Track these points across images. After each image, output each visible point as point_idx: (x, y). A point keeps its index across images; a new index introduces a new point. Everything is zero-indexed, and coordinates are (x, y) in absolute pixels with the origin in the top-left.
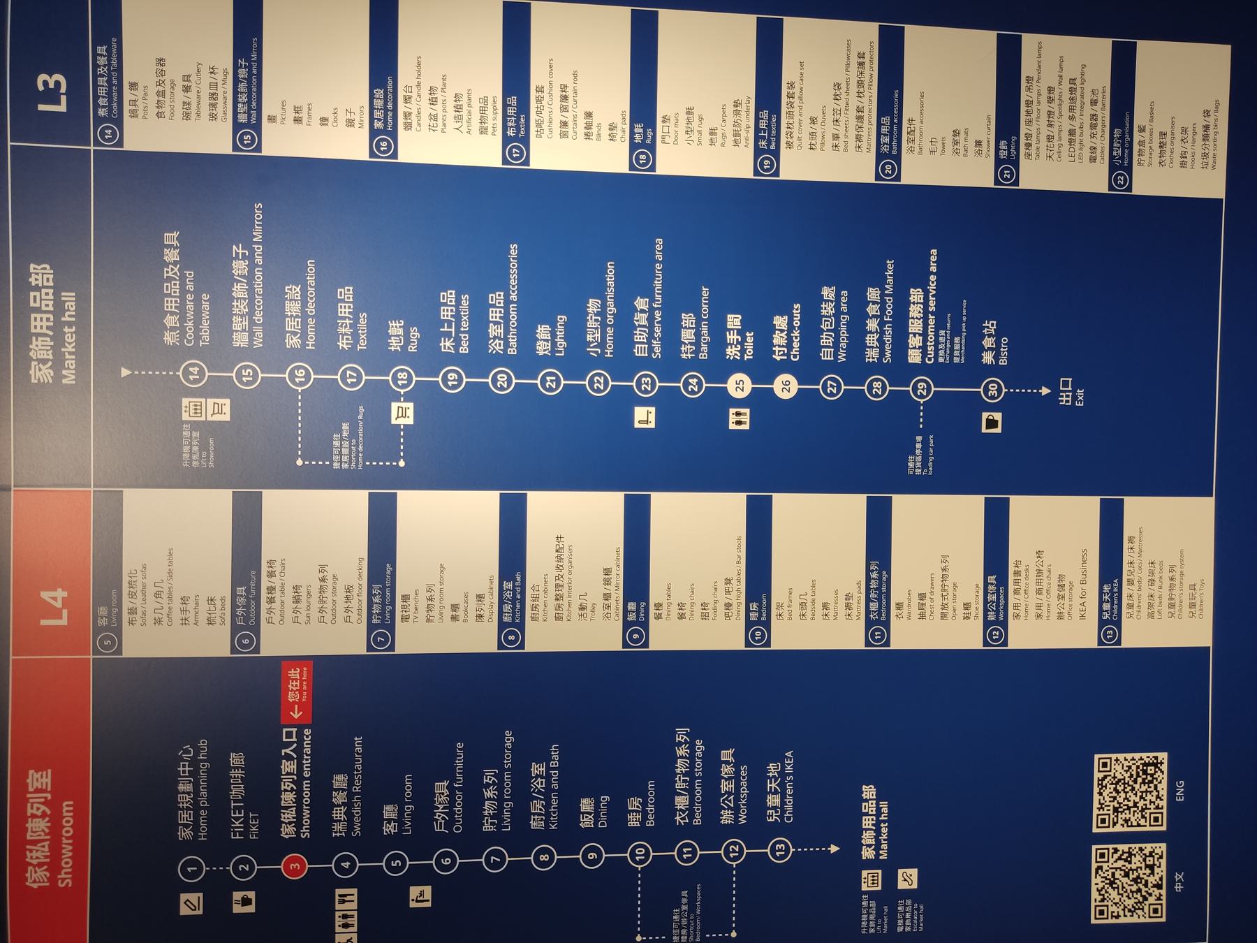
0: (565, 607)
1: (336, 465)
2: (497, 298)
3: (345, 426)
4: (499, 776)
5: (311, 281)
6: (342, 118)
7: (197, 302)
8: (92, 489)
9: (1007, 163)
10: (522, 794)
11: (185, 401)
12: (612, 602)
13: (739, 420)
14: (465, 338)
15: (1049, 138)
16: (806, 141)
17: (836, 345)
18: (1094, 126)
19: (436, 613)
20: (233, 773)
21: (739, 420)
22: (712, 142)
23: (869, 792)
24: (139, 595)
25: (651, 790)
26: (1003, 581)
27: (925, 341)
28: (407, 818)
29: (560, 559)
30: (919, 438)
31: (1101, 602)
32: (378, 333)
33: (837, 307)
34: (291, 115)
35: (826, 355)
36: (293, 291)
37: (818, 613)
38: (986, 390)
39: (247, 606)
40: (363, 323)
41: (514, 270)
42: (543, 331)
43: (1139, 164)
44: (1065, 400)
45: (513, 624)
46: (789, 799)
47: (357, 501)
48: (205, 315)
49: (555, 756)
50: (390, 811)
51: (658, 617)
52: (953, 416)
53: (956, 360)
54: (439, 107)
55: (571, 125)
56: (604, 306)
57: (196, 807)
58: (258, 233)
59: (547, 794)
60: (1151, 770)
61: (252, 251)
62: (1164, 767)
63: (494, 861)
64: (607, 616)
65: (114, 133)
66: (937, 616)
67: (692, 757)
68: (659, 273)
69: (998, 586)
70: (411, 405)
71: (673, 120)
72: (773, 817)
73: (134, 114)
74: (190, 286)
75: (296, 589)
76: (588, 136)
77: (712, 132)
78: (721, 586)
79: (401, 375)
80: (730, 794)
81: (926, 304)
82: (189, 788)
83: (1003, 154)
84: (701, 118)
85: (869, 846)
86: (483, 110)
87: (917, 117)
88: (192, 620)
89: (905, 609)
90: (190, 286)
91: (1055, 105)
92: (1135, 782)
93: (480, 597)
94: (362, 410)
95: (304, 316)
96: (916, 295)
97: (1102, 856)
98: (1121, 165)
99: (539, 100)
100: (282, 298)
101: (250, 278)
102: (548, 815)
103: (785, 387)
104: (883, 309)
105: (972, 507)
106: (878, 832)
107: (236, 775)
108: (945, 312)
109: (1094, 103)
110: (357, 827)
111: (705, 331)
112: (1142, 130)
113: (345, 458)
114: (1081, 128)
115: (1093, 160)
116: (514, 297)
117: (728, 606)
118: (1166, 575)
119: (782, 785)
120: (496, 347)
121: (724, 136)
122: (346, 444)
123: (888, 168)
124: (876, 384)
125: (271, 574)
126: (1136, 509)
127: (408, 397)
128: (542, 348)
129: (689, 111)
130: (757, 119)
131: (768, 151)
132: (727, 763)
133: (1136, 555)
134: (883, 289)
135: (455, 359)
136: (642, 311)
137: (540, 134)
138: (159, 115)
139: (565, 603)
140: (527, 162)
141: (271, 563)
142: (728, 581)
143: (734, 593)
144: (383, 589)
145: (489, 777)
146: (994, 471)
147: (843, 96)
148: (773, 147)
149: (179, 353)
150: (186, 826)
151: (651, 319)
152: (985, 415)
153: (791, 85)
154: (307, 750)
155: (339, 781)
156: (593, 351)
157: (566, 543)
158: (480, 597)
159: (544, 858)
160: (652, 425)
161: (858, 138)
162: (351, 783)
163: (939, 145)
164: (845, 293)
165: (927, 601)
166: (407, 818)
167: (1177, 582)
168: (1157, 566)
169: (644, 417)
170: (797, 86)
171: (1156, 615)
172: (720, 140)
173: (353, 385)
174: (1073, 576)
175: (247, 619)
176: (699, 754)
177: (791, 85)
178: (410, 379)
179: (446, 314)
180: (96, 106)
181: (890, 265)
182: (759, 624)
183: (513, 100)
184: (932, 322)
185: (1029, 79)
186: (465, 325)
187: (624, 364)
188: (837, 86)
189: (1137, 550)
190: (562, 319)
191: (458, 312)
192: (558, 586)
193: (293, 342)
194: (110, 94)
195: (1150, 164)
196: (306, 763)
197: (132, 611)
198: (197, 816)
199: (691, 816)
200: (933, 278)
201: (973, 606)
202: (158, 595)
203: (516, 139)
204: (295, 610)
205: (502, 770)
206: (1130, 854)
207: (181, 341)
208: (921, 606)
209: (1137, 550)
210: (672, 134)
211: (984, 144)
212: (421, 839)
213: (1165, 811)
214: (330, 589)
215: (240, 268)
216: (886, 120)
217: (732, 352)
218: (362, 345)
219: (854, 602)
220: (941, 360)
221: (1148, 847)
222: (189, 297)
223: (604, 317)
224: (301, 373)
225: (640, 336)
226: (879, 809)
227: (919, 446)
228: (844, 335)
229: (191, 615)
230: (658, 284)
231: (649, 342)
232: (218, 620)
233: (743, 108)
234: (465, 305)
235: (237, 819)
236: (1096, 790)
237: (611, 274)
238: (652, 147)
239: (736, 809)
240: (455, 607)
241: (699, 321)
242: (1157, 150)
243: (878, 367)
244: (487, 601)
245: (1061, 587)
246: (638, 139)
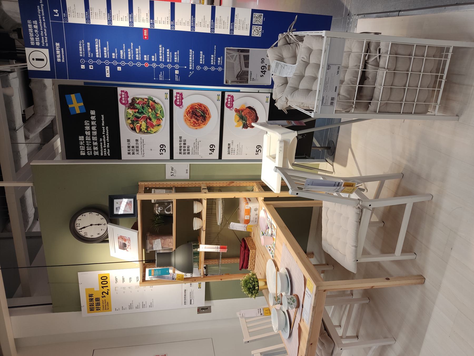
50: (113, 54)
59: (139, 53)
63: (131, 64)
72: (176, 61)
107: (89, 46)
155: (105, 48)
159: (139, 65)
196: (100, 45)
212: (119, 60)
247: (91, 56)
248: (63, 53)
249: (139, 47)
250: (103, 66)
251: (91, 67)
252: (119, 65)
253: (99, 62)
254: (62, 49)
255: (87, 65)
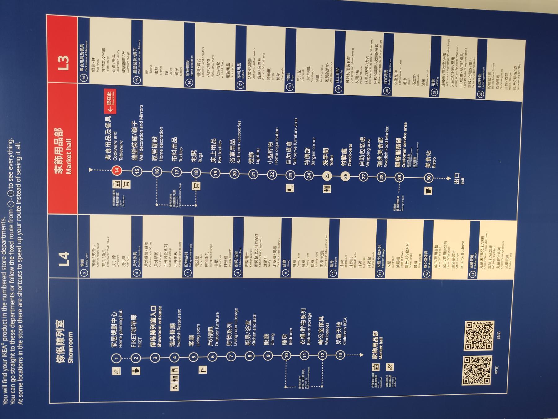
0: (258, 261)
1: (171, 206)
2: (233, 142)
3: (174, 191)
4: (233, 325)
5: (162, 135)
6: (174, 72)
7: (118, 144)
8: (78, 214)
9: (435, 88)
10: (242, 333)
11: (114, 181)
12: (277, 259)
13: (327, 189)
14: (220, 157)
15: (452, 78)
16: (354, 80)
17: (365, 160)
18: (470, 73)
19: (209, 263)
20: (132, 322)
21: (327, 189)
22: (317, 80)
23: (375, 333)
24: (96, 255)
25: (291, 332)
26: (430, 253)
27: (402, 158)
28: (198, 340)
29: (256, 243)
30: (398, 197)
31: (469, 262)
32: (187, 156)
33: (366, 145)
34: (153, 70)
35: (362, 164)
36: (155, 139)
37: (356, 266)
38: (426, 178)
39: (137, 260)
40: (181, 151)
41: (239, 131)
42: (251, 155)
43: (489, 88)
44: (457, 182)
45: (238, 268)
46: (345, 336)
47: (178, 220)
48: (121, 148)
49: (255, 318)
50: (191, 337)
51: (294, 265)
52: (412, 189)
53: (414, 166)
54: (211, 67)
55: (262, 74)
56: (274, 145)
57: (118, 335)
58: (141, 117)
59: (251, 332)
60: (488, 327)
61: (139, 124)
62: (493, 326)
63: (231, 357)
64: (275, 265)
65: (86, 78)
66: (404, 267)
67: (307, 319)
68: (296, 132)
69: (428, 255)
70: (199, 183)
71: (302, 72)
72: (338, 342)
73: (93, 70)
74: (115, 138)
75: (156, 253)
76: (268, 78)
77: (317, 76)
78: (319, 254)
79: (196, 171)
80: (322, 333)
81: (402, 144)
82: (116, 328)
83: (433, 84)
84: (313, 71)
85: (375, 354)
86: (228, 68)
87: (399, 70)
88: (116, 265)
89: (391, 263)
90: (115, 138)
91: (455, 64)
92: (481, 332)
93: (226, 257)
94: (180, 184)
95: (159, 149)
96: (399, 140)
97: (467, 360)
98: (481, 88)
99: (250, 64)
100: (150, 142)
101: (138, 134)
102: (252, 340)
103: (345, 176)
104: (384, 146)
105: (418, 224)
106: (379, 349)
107: (133, 323)
108: (410, 147)
109: (470, 63)
110: (179, 343)
111: (314, 155)
112: (490, 74)
113: (174, 203)
114: (465, 74)
115: (470, 86)
116: (239, 141)
117: (322, 262)
118: (496, 251)
119: (342, 330)
120: (232, 160)
121: (322, 78)
122: (174, 198)
123: (387, 90)
124: (381, 176)
125: (146, 248)
126: (486, 226)
127: (198, 180)
128: (251, 161)
129: (308, 68)
130: (335, 71)
131: (339, 84)
132: (321, 322)
133: (484, 243)
134: (384, 138)
135: (216, 165)
136: (289, 147)
137: (250, 77)
138: (103, 70)
139: (258, 260)
140: (245, 89)
141: (146, 243)
142: (322, 252)
143: (324, 257)
144: (189, 254)
145: (229, 325)
146: (428, 210)
147: (369, 62)
148: (341, 82)
149: (111, 163)
150: (114, 342)
151: (293, 150)
152: (426, 188)
153: (349, 58)
154: (160, 314)
155: (172, 326)
156: (270, 162)
157: (259, 236)
158: (226, 257)
159: (250, 356)
160: (293, 191)
161: (375, 79)
162: (177, 327)
163: (407, 81)
164: (369, 139)
165: (400, 261)
166: (198, 340)
167: (501, 254)
168: (493, 248)
169: (290, 188)
170: (351, 58)
171: (492, 267)
172: (320, 80)
173: (177, 175)
174: (459, 251)
175: (137, 264)
176: (310, 318)
177: (349, 58)
178: (199, 173)
179: (213, 148)
180: (79, 67)
181: (387, 129)
182: (333, 269)
183: (239, 65)
184: (405, 151)
185: (444, 54)
186: (220, 152)
187: (282, 167)
188: (367, 58)
189: (485, 241)
190: (258, 150)
191: (217, 147)
192: (256, 253)
193: (154, 158)
194: (84, 62)
195: (493, 88)
196: (160, 319)
197: (94, 261)
198: (118, 339)
199: (306, 341)
200: (405, 134)
201: (418, 263)
202: (103, 255)
203: (240, 79)
204: (155, 261)
205: (234, 323)
206: (478, 360)
207: (112, 159)
208: (398, 262)
209: (485, 241)
210: (301, 77)
211: (426, 80)
213: (492, 343)
214: (168, 253)
215: (134, 130)
216: (386, 71)
217: (325, 163)
218: (181, 159)
219: (371, 261)
220: (408, 166)
221: (485, 357)
222: (115, 142)
223: (274, 149)
224: (157, 170)
225: (288, 156)
226: (379, 340)
227: (398, 200)
228: (369, 156)
229: (116, 263)
230: (295, 136)
231: (292, 159)
232: (126, 265)
233: (330, 67)
234: (220, 144)
235: (133, 340)
236: (466, 335)
237: (277, 132)
238: (294, 83)
239: (324, 339)
240: (216, 261)
241: (311, 150)
242: (495, 82)
243: (382, 169)
244: (228, 258)
245: (454, 255)
246: (288, 79)
247: (137, 345)
248: (71, 342)
249: (254, 316)
250: (165, 366)
251: (136, 372)
252: (203, 362)
253: (155, 358)
254: (70, 334)
255: (126, 367)
